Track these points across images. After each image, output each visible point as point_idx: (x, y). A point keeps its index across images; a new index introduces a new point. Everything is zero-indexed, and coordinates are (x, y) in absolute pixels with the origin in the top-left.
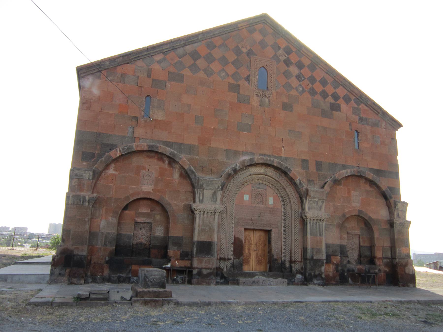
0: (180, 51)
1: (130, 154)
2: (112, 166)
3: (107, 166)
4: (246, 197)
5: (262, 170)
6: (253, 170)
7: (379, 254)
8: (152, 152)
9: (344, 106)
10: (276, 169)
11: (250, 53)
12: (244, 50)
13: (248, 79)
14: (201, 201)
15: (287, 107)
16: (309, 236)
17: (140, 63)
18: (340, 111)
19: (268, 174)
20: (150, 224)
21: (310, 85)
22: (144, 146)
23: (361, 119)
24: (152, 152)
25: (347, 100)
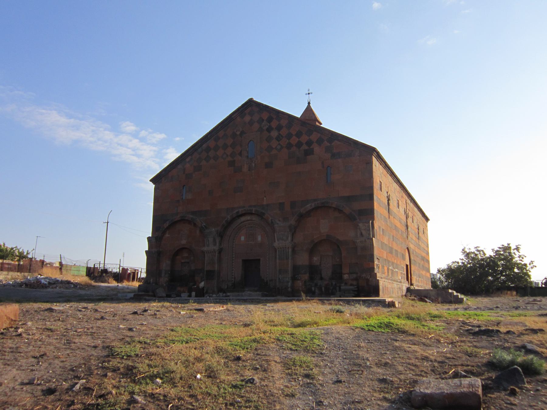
0: (200, 150)
1: (174, 224)
2: (168, 232)
3: (164, 233)
4: (243, 238)
5: (249, 218)
6: (243, 219)
7: (346, 270)
8: (183, 220)
9: (316, 148)
10: (258, 215)
11: (242, 133)
12: (238, 133)
13: (240, 154)
14: (208, 246)
15: (268, 165)
16: (278, 261)
17: (180, 166)
18: (313, 154)
19: (254, 219)
20: (188, 263)
21: (288, 141)
22: (178, 218)
23: (333, 156)
24: (183, 220)
25: (320, 142)
